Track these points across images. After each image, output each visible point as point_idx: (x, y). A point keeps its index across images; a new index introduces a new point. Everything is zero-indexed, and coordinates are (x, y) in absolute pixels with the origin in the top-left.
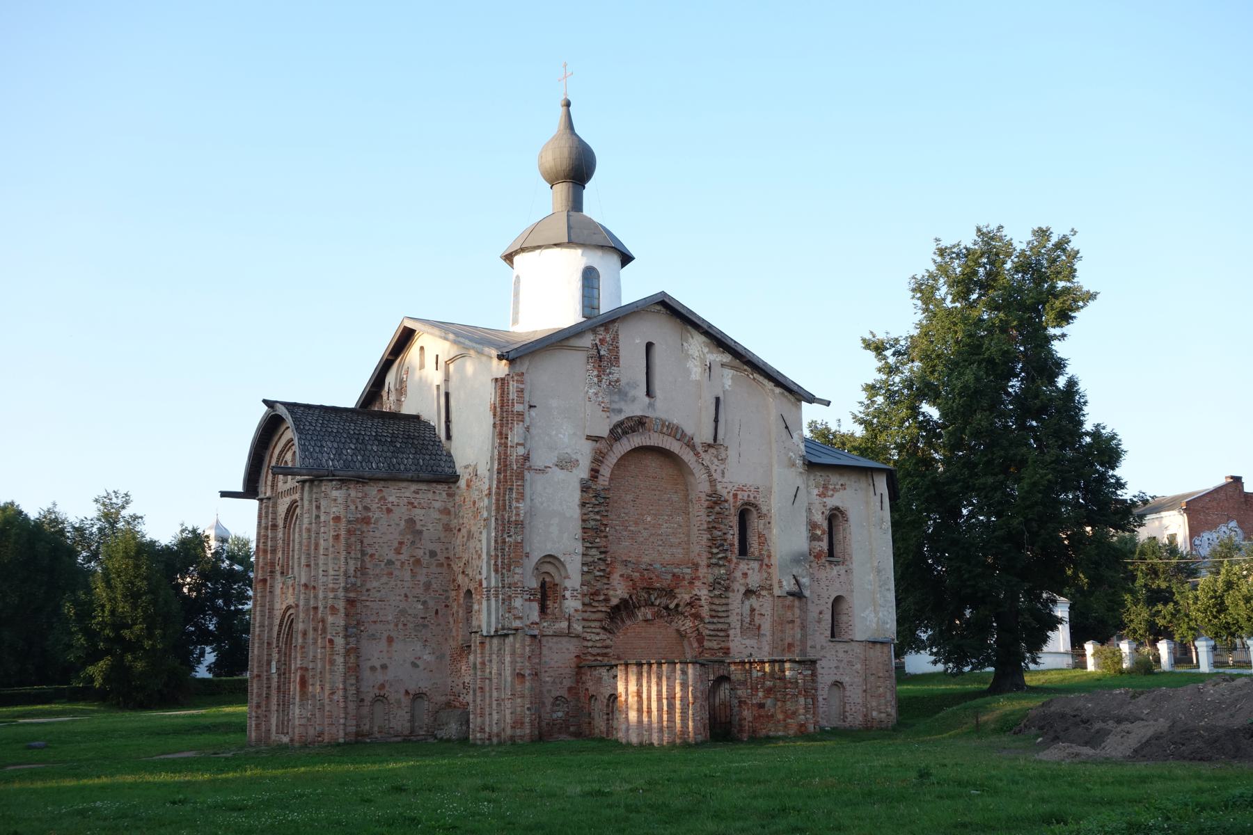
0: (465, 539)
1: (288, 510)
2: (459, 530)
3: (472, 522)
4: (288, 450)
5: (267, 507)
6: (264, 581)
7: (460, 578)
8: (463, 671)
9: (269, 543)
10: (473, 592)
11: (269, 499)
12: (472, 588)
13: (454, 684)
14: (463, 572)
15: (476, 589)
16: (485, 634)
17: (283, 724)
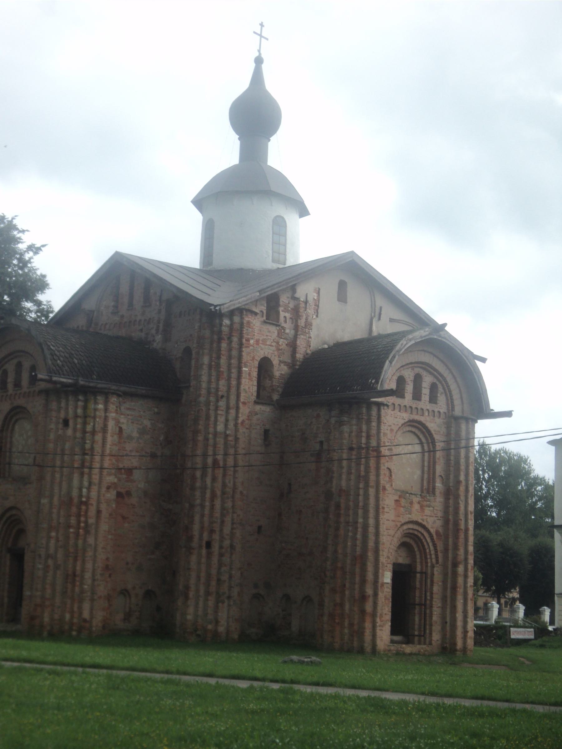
4: (407, 368)
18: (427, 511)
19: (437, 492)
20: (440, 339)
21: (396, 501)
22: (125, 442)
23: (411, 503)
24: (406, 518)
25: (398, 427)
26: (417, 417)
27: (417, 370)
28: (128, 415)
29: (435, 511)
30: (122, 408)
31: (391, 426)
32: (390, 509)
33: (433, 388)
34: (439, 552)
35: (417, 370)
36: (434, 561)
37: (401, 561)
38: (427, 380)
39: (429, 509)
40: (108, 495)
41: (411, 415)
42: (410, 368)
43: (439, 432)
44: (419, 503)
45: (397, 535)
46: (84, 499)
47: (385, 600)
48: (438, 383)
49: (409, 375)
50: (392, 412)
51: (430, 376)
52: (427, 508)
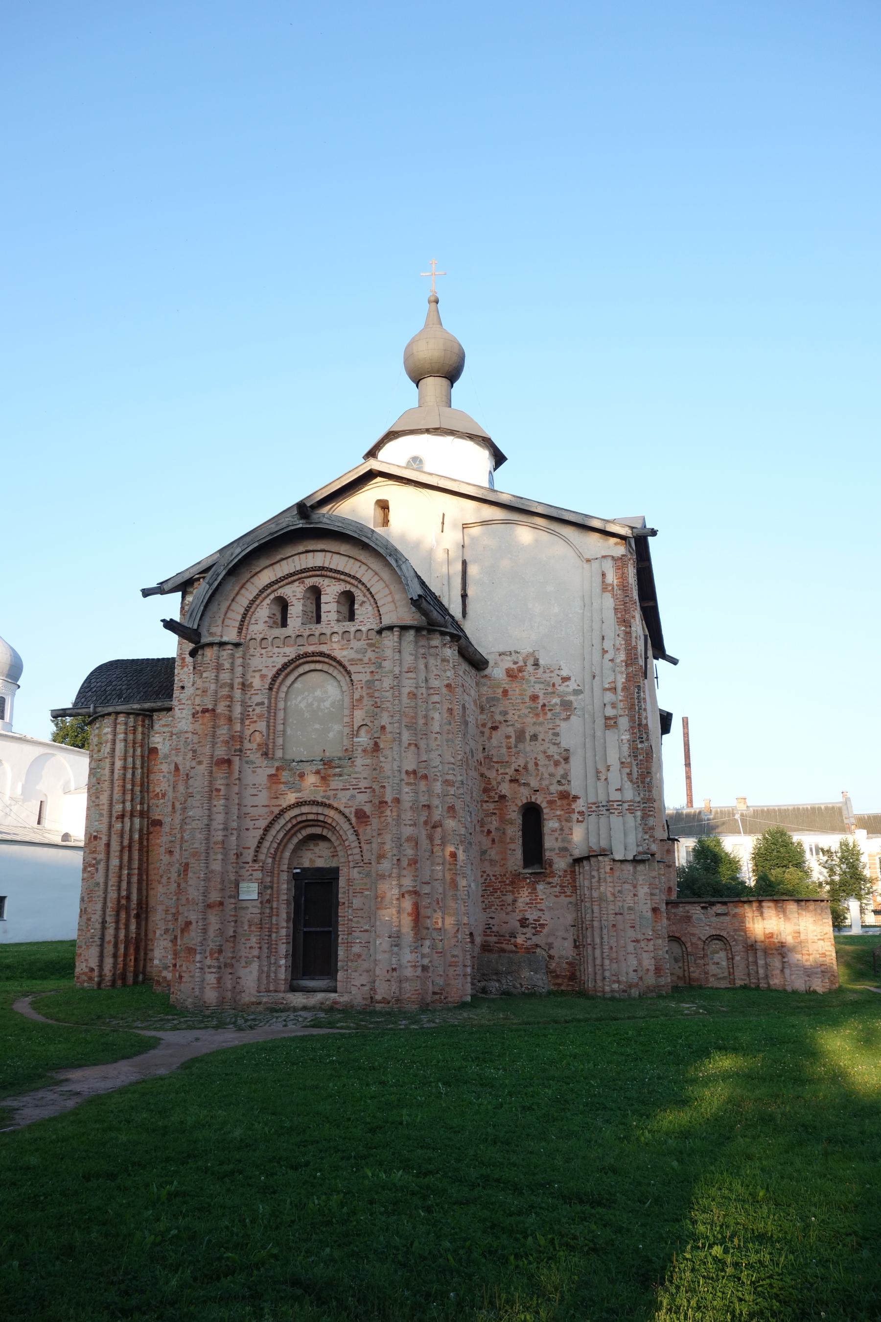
0: (513, 740)
1: (285, 666)
2: (495, 728)
3: (530, 720)
5: (232, 656)
6: (229, 762)
7: (505, 788)
8: (520, 904)
9: (238, 710)
10: (544, 805)
11: (237, 645)
12: (540, 799)
13: (491, 921)
14: (511, 781)
15: (551, 803)
16: (618, 857)
17: (268, 976)
18: (336, 783)
19: (359, 753)
20: (312, 526)
21: (270, 776)
22: (161, 763)
23: (302, 776)
24: (291, 798)
25: (275, 670)
26: (310, 649)
27: (310, 582)
28: (164, 733)
29: (352, 780)
30: (157, 727)
31: (261, 670)
32: (260, 789)
33: (348, 598)
34: (362, 845)
35: (310, 582)
36: (358, 857)
37: (320, 863)
38: (331, 591)
39: (341, 778)
40: (118, 826)
41: (301, 647)
42: (295, 581)
43: (361, 660)
44: (318, 772)
45: (277, 827)
46: (95, 834)
47: (250, 926)
48: (353, 589)
49: (294, 592)
50: (263, 651)
51: (337, 583)
52: (337, 778)
